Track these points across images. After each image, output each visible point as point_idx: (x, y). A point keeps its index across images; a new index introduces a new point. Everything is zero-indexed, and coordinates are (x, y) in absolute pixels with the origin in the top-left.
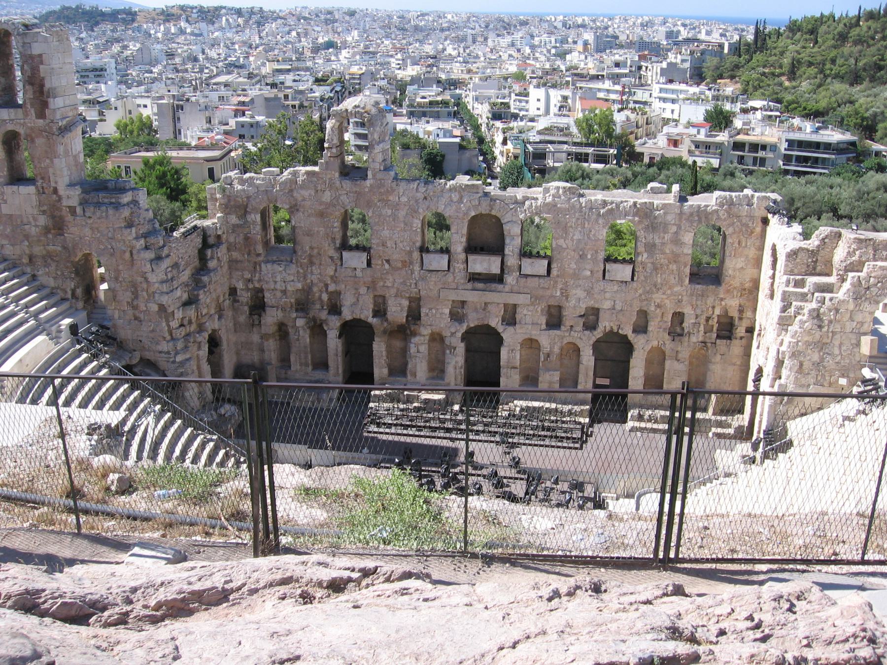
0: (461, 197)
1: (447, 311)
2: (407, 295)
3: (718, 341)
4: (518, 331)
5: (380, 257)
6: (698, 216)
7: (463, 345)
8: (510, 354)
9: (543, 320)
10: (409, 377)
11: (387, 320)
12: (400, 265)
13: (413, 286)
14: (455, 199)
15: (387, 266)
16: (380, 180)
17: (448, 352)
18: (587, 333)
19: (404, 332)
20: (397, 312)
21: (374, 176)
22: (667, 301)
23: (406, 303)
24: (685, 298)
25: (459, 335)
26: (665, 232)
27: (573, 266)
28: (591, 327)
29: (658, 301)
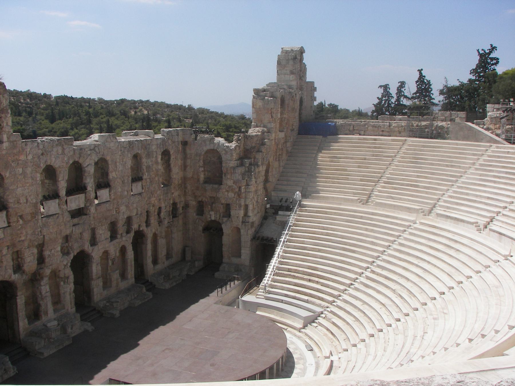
0: (64, 149)
1: (59, 248)
2: (36, 244)
3: (174, 219)
4: (100, 247)
5: (17, 213)
6: (163, 145)
7: (72, 273)
8: (95, 269)
9: (109, 234)
10: (44, 319)
11: (24, 272)
12: (29, 218)
13: (40, 234)
14: (60, 151)
15: (21, 222)
16: (13, 142)
17: (62, 283)
18: (129, 235)
19: (35, 279)
20: (30, 262)
21: (8, 138)
22: (156, 201)
23: (35, 251)
24: (162, 197)
25: (69, 264)
26: (153, 157)
27: (120, 190)
28: (128, 232)
29: (153, 202)
